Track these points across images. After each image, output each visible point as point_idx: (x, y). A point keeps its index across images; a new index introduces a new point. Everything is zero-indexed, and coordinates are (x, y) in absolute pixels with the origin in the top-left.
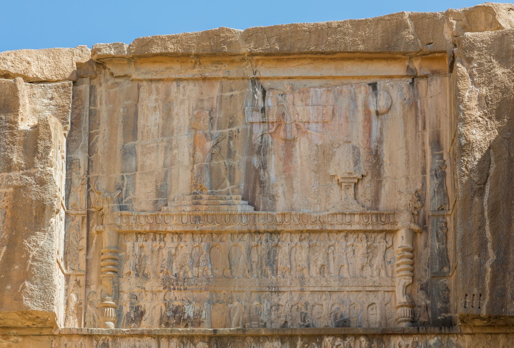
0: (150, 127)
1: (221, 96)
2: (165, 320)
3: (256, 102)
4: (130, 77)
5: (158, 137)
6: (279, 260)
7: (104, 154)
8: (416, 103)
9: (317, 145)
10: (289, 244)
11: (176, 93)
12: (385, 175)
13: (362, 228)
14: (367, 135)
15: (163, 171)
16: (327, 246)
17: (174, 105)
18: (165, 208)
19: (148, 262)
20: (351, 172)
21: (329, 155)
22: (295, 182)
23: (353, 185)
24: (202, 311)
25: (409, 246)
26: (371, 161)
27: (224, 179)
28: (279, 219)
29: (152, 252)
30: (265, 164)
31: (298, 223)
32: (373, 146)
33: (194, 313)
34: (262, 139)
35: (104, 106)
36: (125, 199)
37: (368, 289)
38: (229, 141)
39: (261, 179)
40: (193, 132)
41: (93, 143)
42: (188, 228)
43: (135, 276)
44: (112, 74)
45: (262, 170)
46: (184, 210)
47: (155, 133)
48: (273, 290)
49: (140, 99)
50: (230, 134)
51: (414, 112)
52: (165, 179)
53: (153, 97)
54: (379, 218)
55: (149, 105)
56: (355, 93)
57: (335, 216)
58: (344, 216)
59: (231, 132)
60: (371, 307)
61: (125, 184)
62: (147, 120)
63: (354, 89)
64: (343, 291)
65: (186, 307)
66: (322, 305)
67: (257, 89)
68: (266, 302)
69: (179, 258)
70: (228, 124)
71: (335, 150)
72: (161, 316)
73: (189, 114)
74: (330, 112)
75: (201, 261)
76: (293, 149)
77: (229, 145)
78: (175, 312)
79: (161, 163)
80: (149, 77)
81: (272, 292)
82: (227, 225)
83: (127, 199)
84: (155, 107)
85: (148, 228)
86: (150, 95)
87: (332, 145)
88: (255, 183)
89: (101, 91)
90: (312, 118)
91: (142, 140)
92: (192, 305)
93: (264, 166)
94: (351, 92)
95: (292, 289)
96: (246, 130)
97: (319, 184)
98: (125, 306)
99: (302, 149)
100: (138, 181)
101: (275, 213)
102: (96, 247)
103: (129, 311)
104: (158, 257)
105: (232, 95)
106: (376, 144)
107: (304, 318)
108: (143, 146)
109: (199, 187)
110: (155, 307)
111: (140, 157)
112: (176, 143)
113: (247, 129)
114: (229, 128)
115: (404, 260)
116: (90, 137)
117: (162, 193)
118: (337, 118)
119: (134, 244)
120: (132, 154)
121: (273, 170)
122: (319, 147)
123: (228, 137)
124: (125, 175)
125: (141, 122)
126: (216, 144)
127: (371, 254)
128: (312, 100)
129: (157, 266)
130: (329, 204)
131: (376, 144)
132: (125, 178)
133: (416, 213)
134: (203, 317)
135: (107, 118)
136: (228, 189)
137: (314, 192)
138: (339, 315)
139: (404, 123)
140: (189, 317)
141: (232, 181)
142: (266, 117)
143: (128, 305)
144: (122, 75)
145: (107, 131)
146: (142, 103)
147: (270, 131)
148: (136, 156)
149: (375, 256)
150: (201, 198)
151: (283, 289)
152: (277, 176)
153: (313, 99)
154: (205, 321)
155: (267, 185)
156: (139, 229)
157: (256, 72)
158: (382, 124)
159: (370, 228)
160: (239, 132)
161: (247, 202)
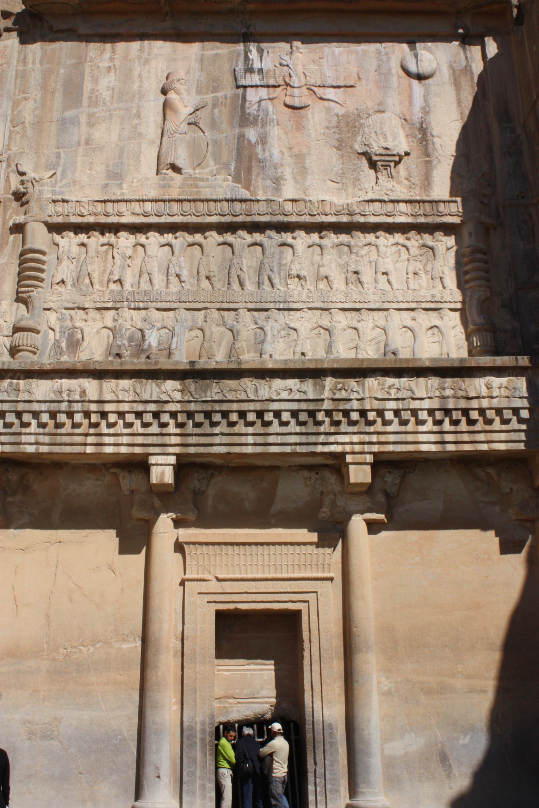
0: (100, 91)
1: (202, 55)
2: (115, 351)
3: (251, 62)
4: (76, 31)
5: (112, 104)
6: (289, 264)
7: (34, 124)
8: (471, 67)
9: (337, 115)
10: (302, 243)
11: (139, 50)
12: (436, 154)
13: (410, 220)
14: (407, 103)
15: (117, 145)
16: (360, 244)
17: (136, 65)
18: (119, 192)
19: (90, 268)
20: (388, 147)
21: (355, 127)
22: (308, 161)
23: (392, 164)
24: (172, 338)
25: (481, 245)
26: (414, 135)
27: (205, 157)
28: (288, 207)
29: (98, 252)
30: (266, 138)
31: (316, 213)
32: (417, 115)
33: (159, 341)
34: (259, 106)
35: (38, 65)
36: (61, 180)
37: (424, 305)
38: (212, 109)
39: (260, 156)
40: (162, 98)
41: (19, 111)
42: (153, 220)
43: (69, 287)
44: (51, 28)
45: (260, 146)
46: (146, 195)
47: (108, 98)
48: (281, 306)
49: (88, 59)
50: (213, 101)
51: (468, 77)
52: (121, 155)
53: (107, 55)
54: (434, 208)
55: (101, 65)
56: (387, 54)
57: (370, 204)
58: (383, 204)
59: (215, 99)
60: (430, 332)
61: (62, 162)
62: (97, 83)
63: (385, 48)
64: (387, 310)
65: (146, 331)
66: (355, 329)
67: (251, 48)
68: (270, 324)
69: (137, 263)
70: (211, 88)
71: (362, 121)
72: (108, 345)
73: (157, 76)
74: (355, 75)
75: (171, 265)
76: (304, 120)
77: (212, 114)
78: (131, 339)
79: (114, 137)
80: (102, 30)
81: (279, 309)
82: (210, 216)
83: (64, 182)
84: (110, 67)
85: (91, 219)
86: (102, 53)
87: (359, 115)
88: (250, 161)
89: (35, 48)
90: (330, 82)
91: (89, 107)
92: (155, 329)
93: (263, 140)
94: (379, 53)
95: (310, 305)
96: (237, 95)
97: (343, 164)
98: (53, 330)
99: (316, 118)
100: (80, 158)
101: (281, 200)
102: (13, 246)
103: (57, 338)
104: (106, 259)
105: (217, 54)
106: (420, 115)
107: (330, 347)
108: (91, 116)
109: (169, 166)
110: (98, 332)
111: (84, 128)
112: (138, 111)
113: (238, 95)
114: (212, 92)
115: (476, 264)
116: (16, 104)
117: (115, 175)
118: (364, 82)
119: (70, 242)
120: (73, 124)
121: (276, 145)
122: (340, 118)
123: (210, 103)
124: (61, 151)
125: (88, 86)
126: (194, 112)
127: (424, 257)
128: (327, 61)
129: (103, 274)
130: (360, 190)
131: (420, 115)
132: (63, 155)
133: (486, 201)
134: (174, 346)
135: (41, 80)
136: (212, 170)
137: (336, 174)
138: (382, 345)
139: (457, 90)
140: (150, 346)
141: (217, 159)
142: (265, 80)
143: (57, 329)
144: (64, 27)
145: (39, 96)
146: (91, 63)
147: (271, 96)
148: (79, 127)
149: (430, 259)
150: (172, 179)
151: (294, 306)
152: (282, 153)
153: (330, 59)
154: (176, 353)
155: (267, 164)
156: (79, 220)
157: (249, 26)
158: (426, 90)
159: (422, 220)
160: (226, 98)
161: (239, 186)
